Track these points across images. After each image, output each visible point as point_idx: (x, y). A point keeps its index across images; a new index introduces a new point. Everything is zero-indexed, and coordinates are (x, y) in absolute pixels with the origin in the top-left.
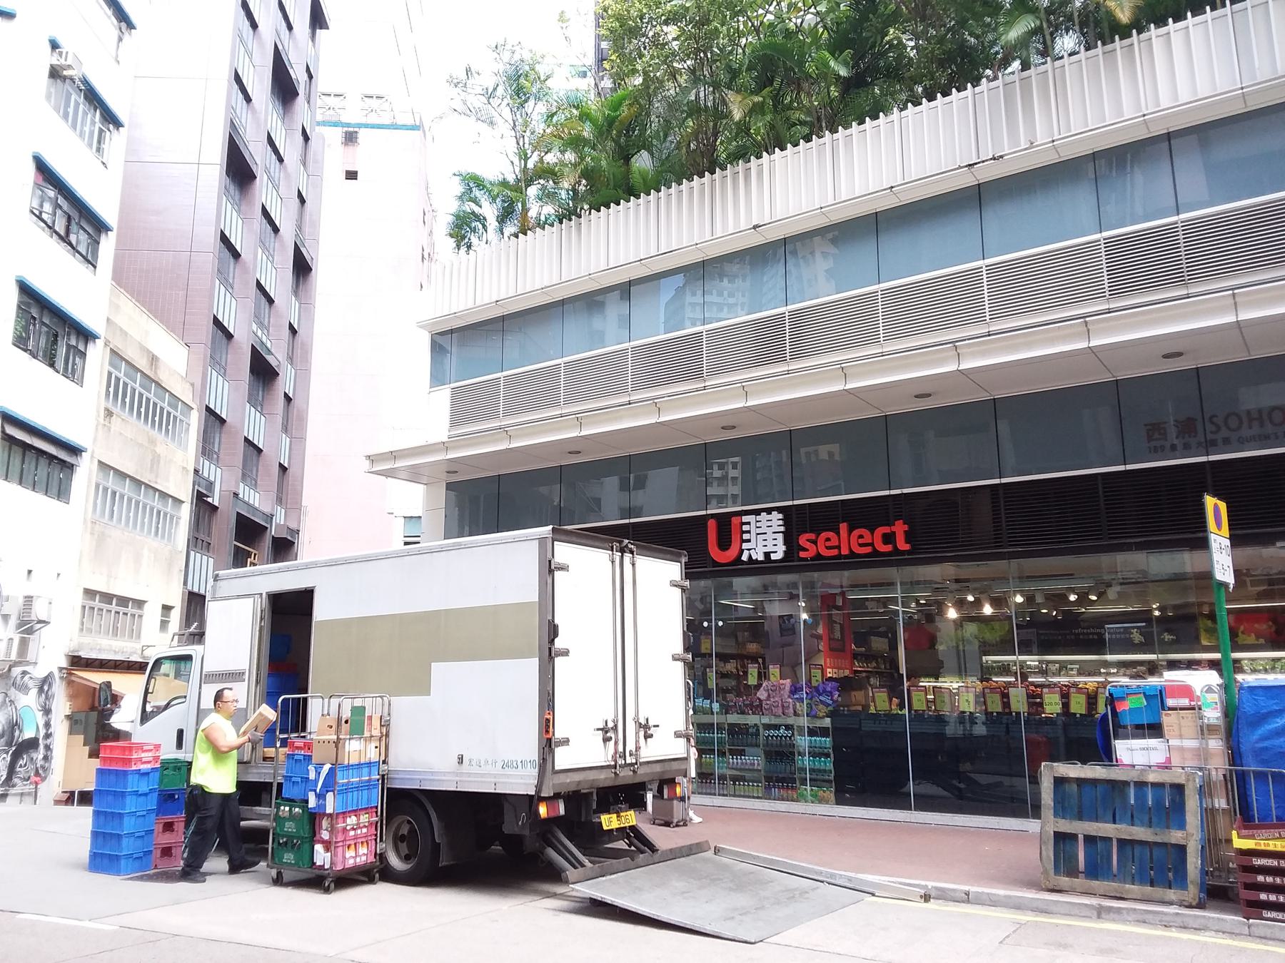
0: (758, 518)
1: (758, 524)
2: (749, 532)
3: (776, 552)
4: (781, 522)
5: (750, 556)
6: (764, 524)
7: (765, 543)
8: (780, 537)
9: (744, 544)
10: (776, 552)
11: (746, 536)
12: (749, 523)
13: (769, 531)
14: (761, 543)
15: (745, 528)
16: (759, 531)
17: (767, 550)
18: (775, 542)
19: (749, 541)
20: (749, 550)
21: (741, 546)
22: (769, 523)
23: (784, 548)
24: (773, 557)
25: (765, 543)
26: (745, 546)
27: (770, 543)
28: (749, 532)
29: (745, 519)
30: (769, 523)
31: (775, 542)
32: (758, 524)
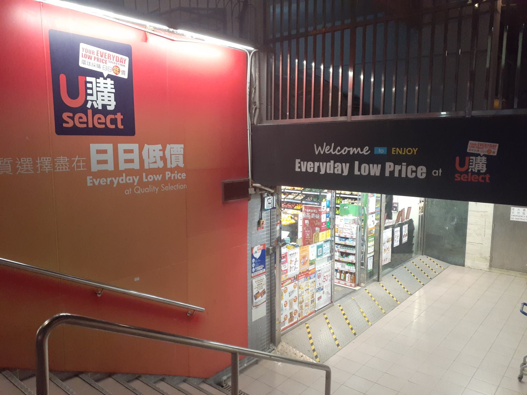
0: (98, 80)
1: (98, 85)
2: (91, 89)
3: (110, 105)
4: (113, 86)
5: (92, 105)
6: (102, 85)
7: (103, 98)
8: (112, 95)
9: (88, 97)
10: (110, 105)
11: (89, 91)
12: (91, 83)
13: (106, 90)
14: (100, 98)
15: (89, 85)
16: (98, 89)
17: (104, 103)
18: (109, 99)
19: (92, 95)
20: (92, 101)
21: (86, 98)
22: (105, 86)
23: (115, 103)
24: (109, 108)
25: (103, 98)
26: (89, 98)
27: (106, 98)
28: (91, 89)
29: (89, 79)
30: (105, 86)
31: (109, 99)
32: (98, 85)
